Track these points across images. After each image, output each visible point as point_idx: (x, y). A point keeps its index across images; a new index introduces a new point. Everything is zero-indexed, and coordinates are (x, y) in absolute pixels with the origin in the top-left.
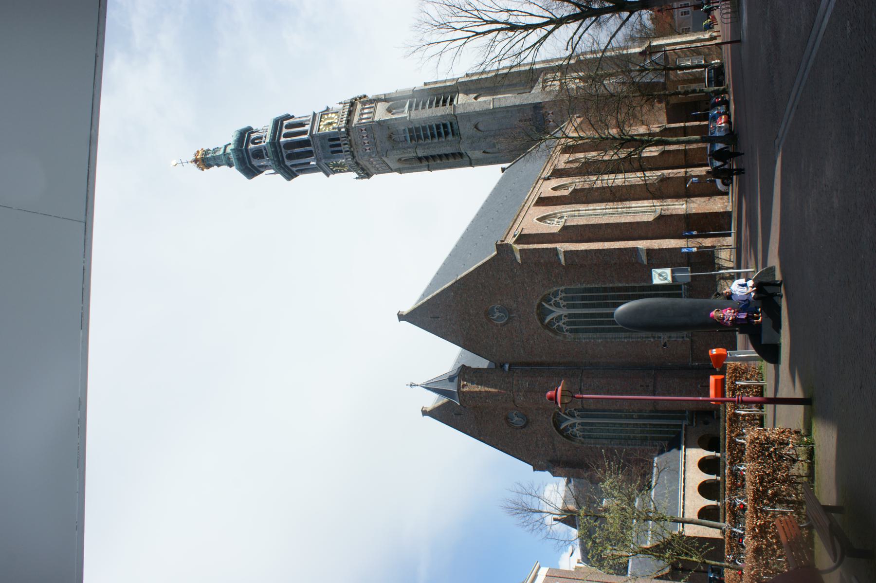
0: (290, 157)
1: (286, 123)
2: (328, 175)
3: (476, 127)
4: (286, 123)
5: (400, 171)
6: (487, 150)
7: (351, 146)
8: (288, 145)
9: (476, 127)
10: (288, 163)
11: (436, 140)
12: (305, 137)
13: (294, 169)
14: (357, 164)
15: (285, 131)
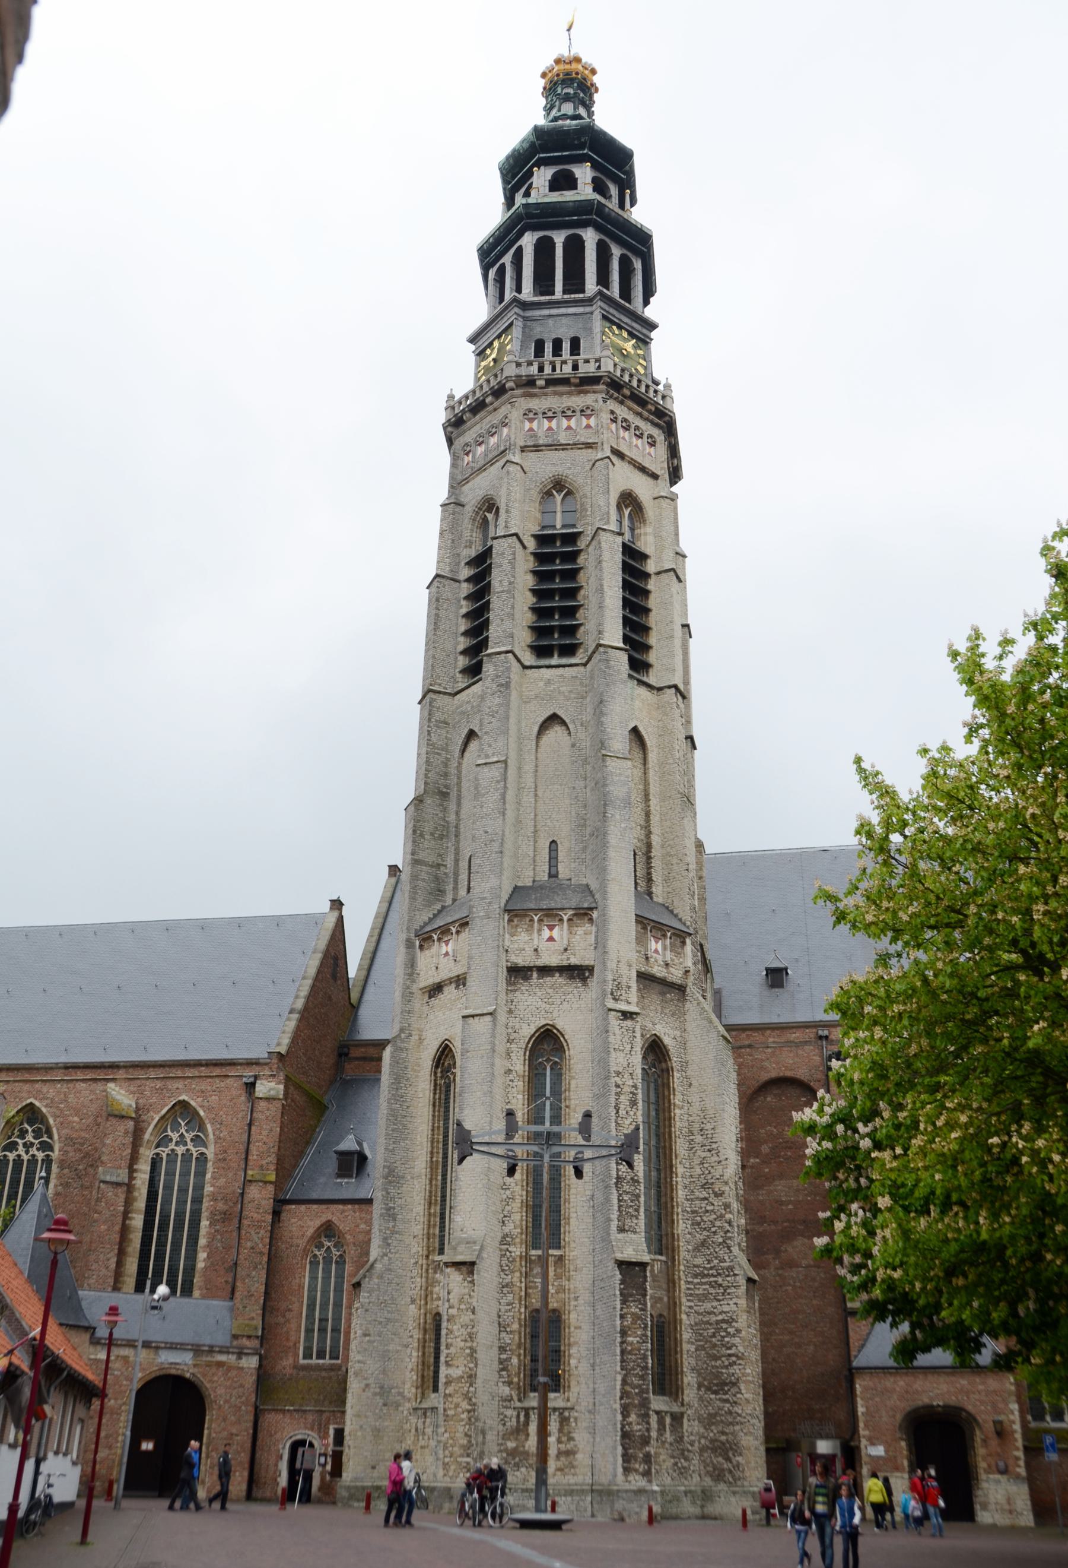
0: (544, 249)
1: (638, 265)
2: (473, 340)
3: (554, 719)
4: (638, 265)
5: (453, 505)
6: (473, 745)
7: (551, 382)
8: (575, 247)
9: (554, 719)
10: (528, 241)
11: (531, 600)
12: (591, 285)
13: (507, 259)
14: (499, 392)
15: (616, 251)
